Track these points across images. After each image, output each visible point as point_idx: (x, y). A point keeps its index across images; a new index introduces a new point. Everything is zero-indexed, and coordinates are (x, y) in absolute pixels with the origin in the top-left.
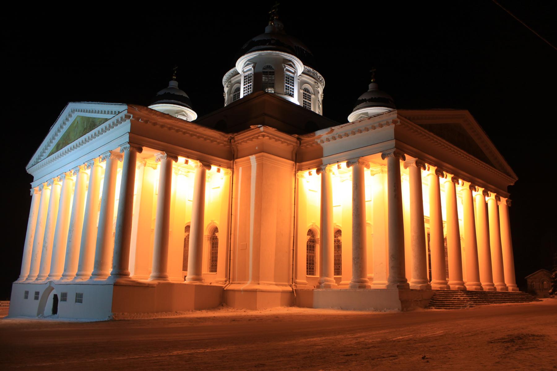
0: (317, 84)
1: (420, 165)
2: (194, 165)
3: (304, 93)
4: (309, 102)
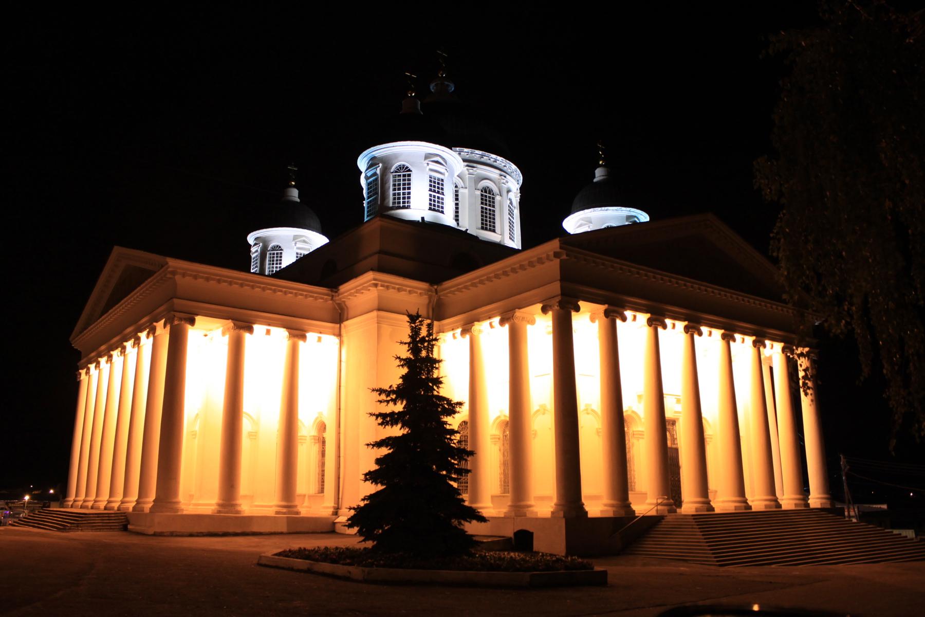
1: (613, 314)
2: (280, 334)
3: (482, 195)
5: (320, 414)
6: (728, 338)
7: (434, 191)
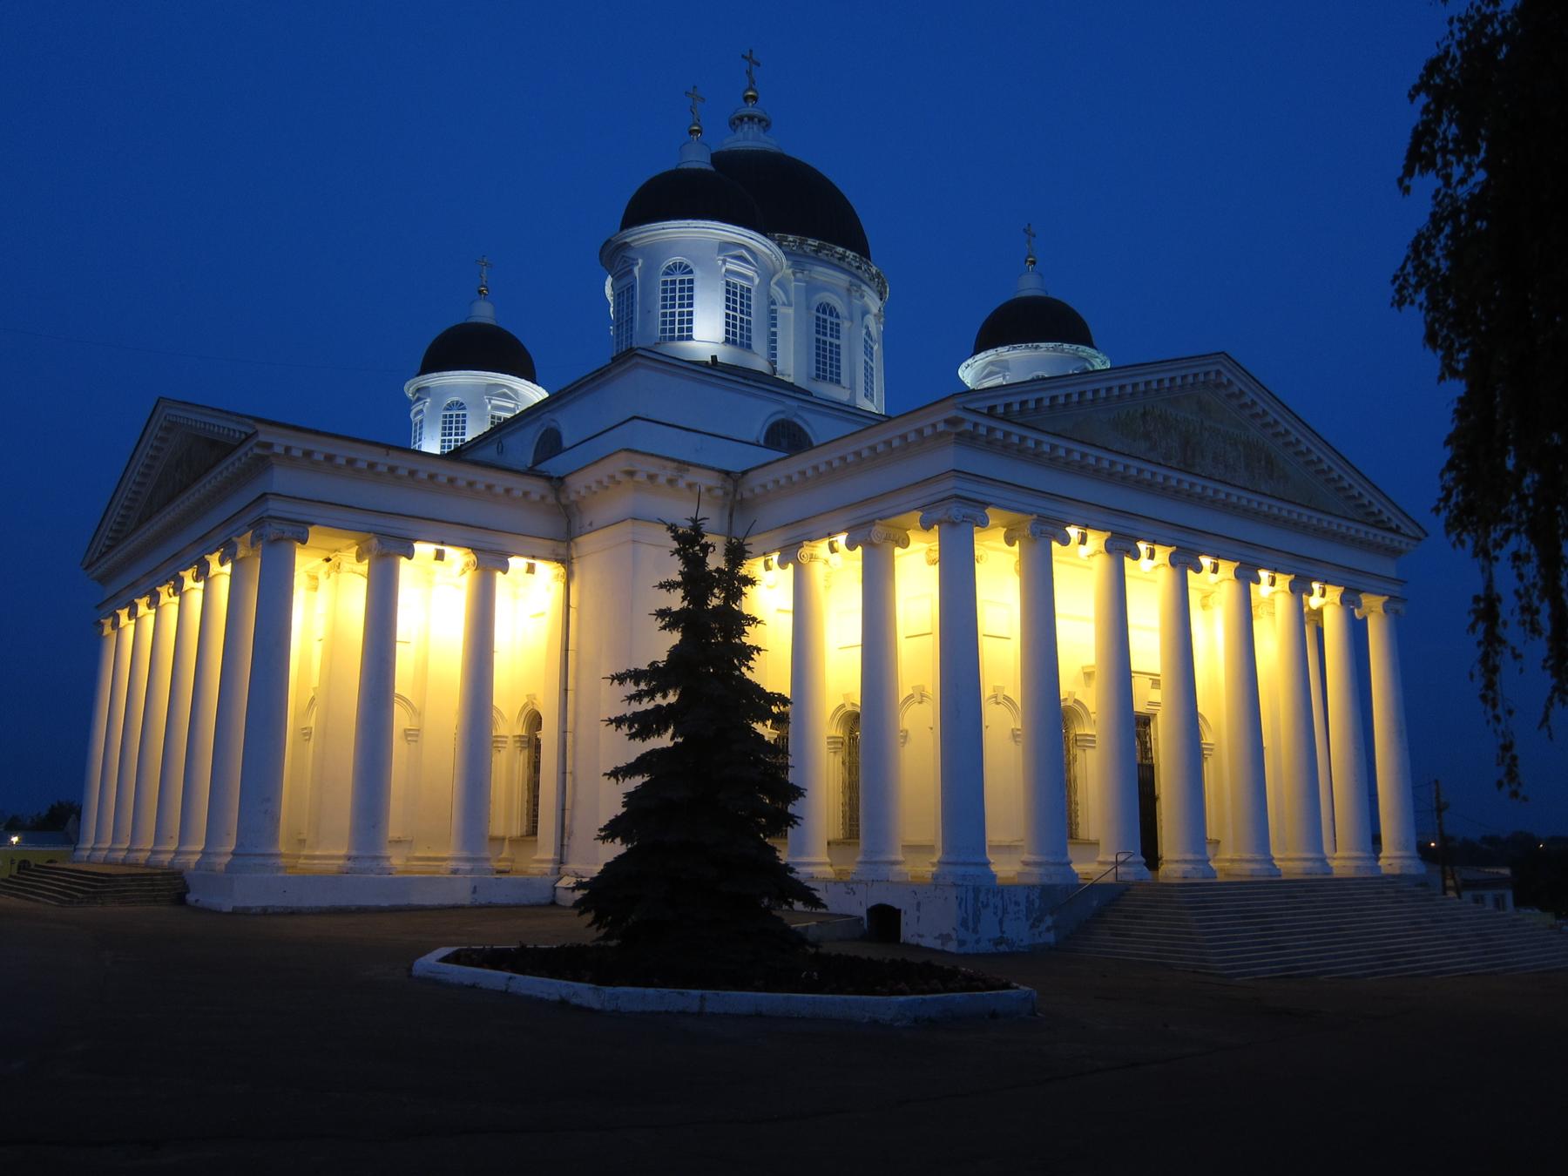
0: (860, 287)
2: (459, 557)
4: (836, 342)
5: (532, 698)
6: (1246, 576)
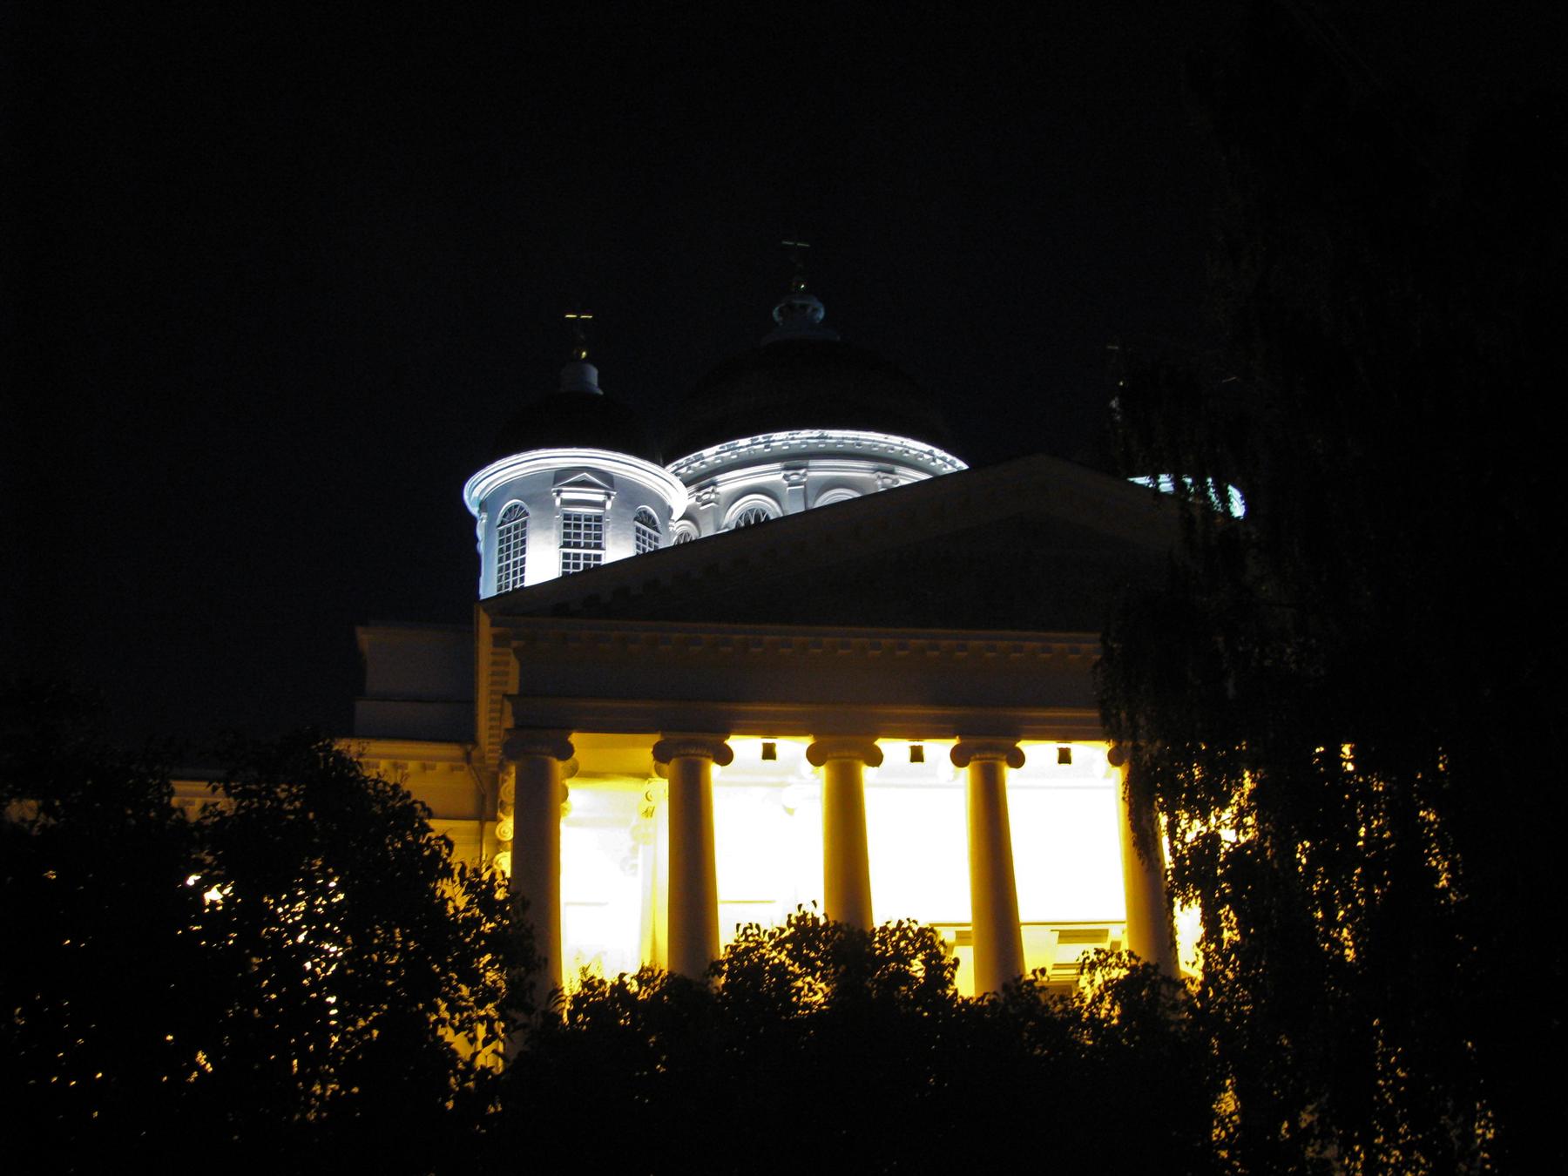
7: (577, 545)
